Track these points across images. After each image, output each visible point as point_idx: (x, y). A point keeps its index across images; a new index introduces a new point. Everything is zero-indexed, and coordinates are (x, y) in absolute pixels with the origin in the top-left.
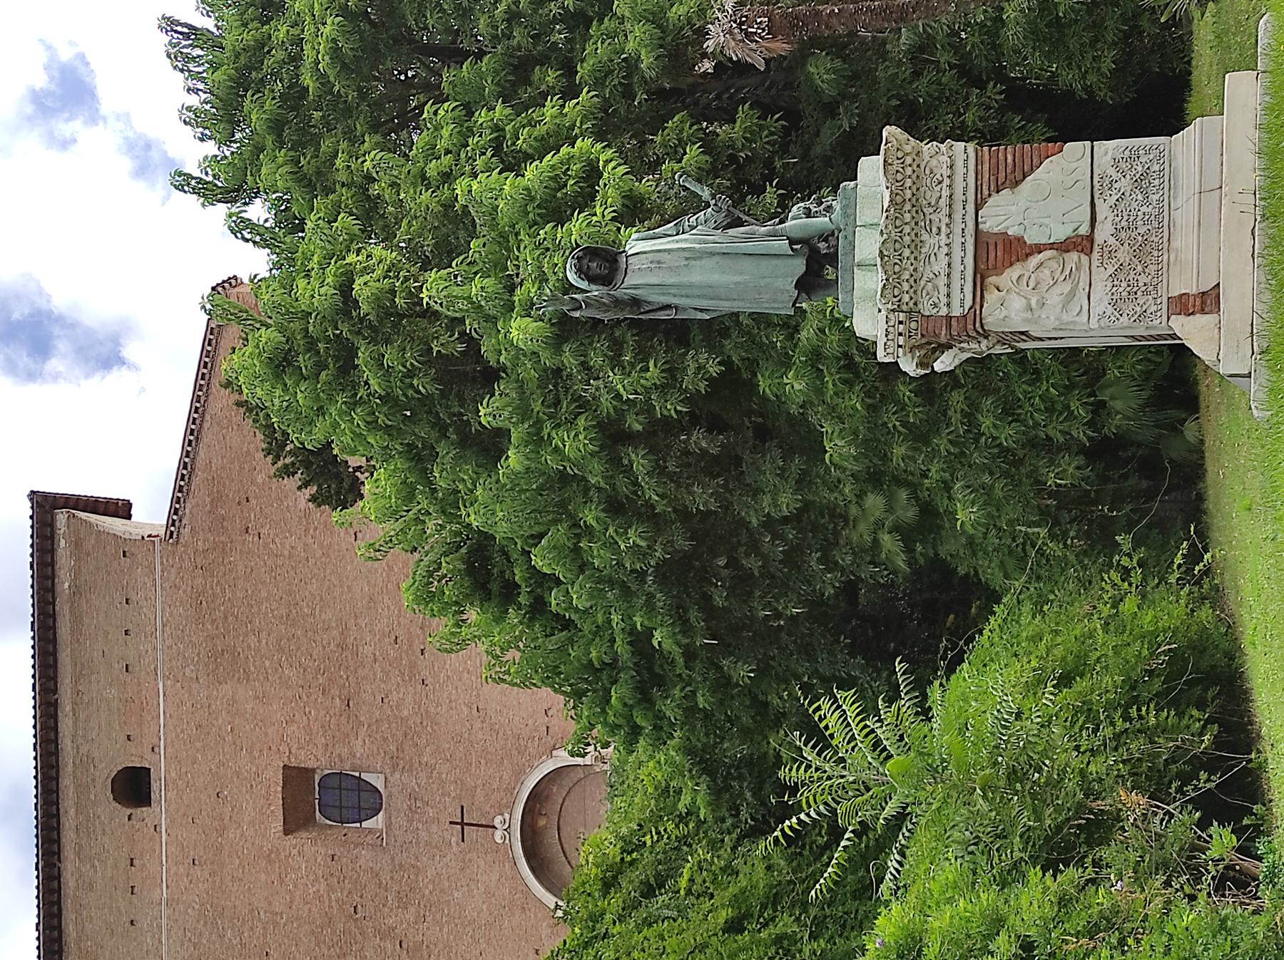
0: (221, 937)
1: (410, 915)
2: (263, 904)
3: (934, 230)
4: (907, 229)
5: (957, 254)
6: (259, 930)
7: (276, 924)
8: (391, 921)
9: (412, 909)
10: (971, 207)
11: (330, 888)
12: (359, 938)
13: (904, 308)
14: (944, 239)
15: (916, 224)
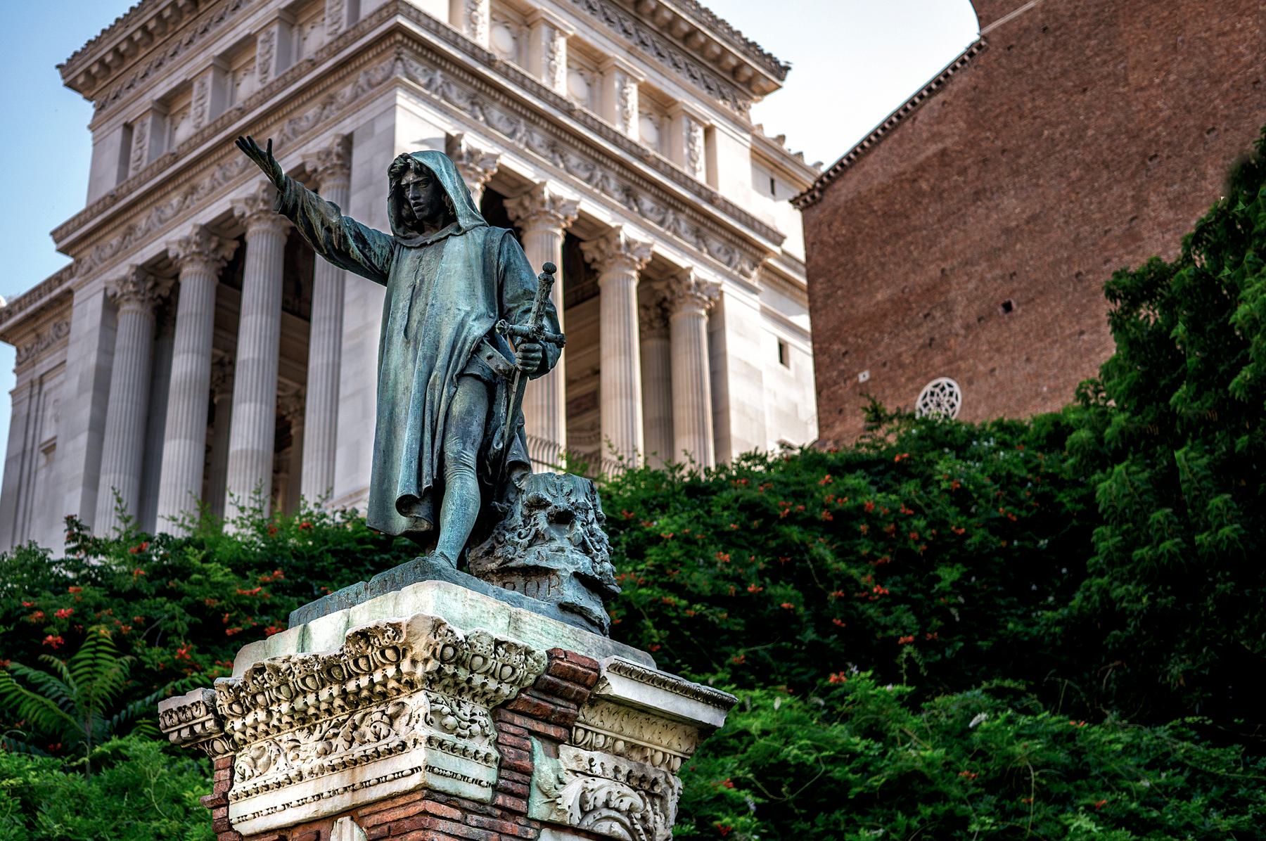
0: (1088, 37)
1: (1166, 215)
2: (1131, 62)
3: (320, 746)
4: (311, 699)
5: (292, 793)
6: (1105, 71)
7: (1116, 84)
8: (1153, 198)
9: (1171, 215)
10: (345, 801)
11: (1167, 122)
12: (1128, 173)
13: (228, 728)
14: (306, 768)
15: (329, 712)
